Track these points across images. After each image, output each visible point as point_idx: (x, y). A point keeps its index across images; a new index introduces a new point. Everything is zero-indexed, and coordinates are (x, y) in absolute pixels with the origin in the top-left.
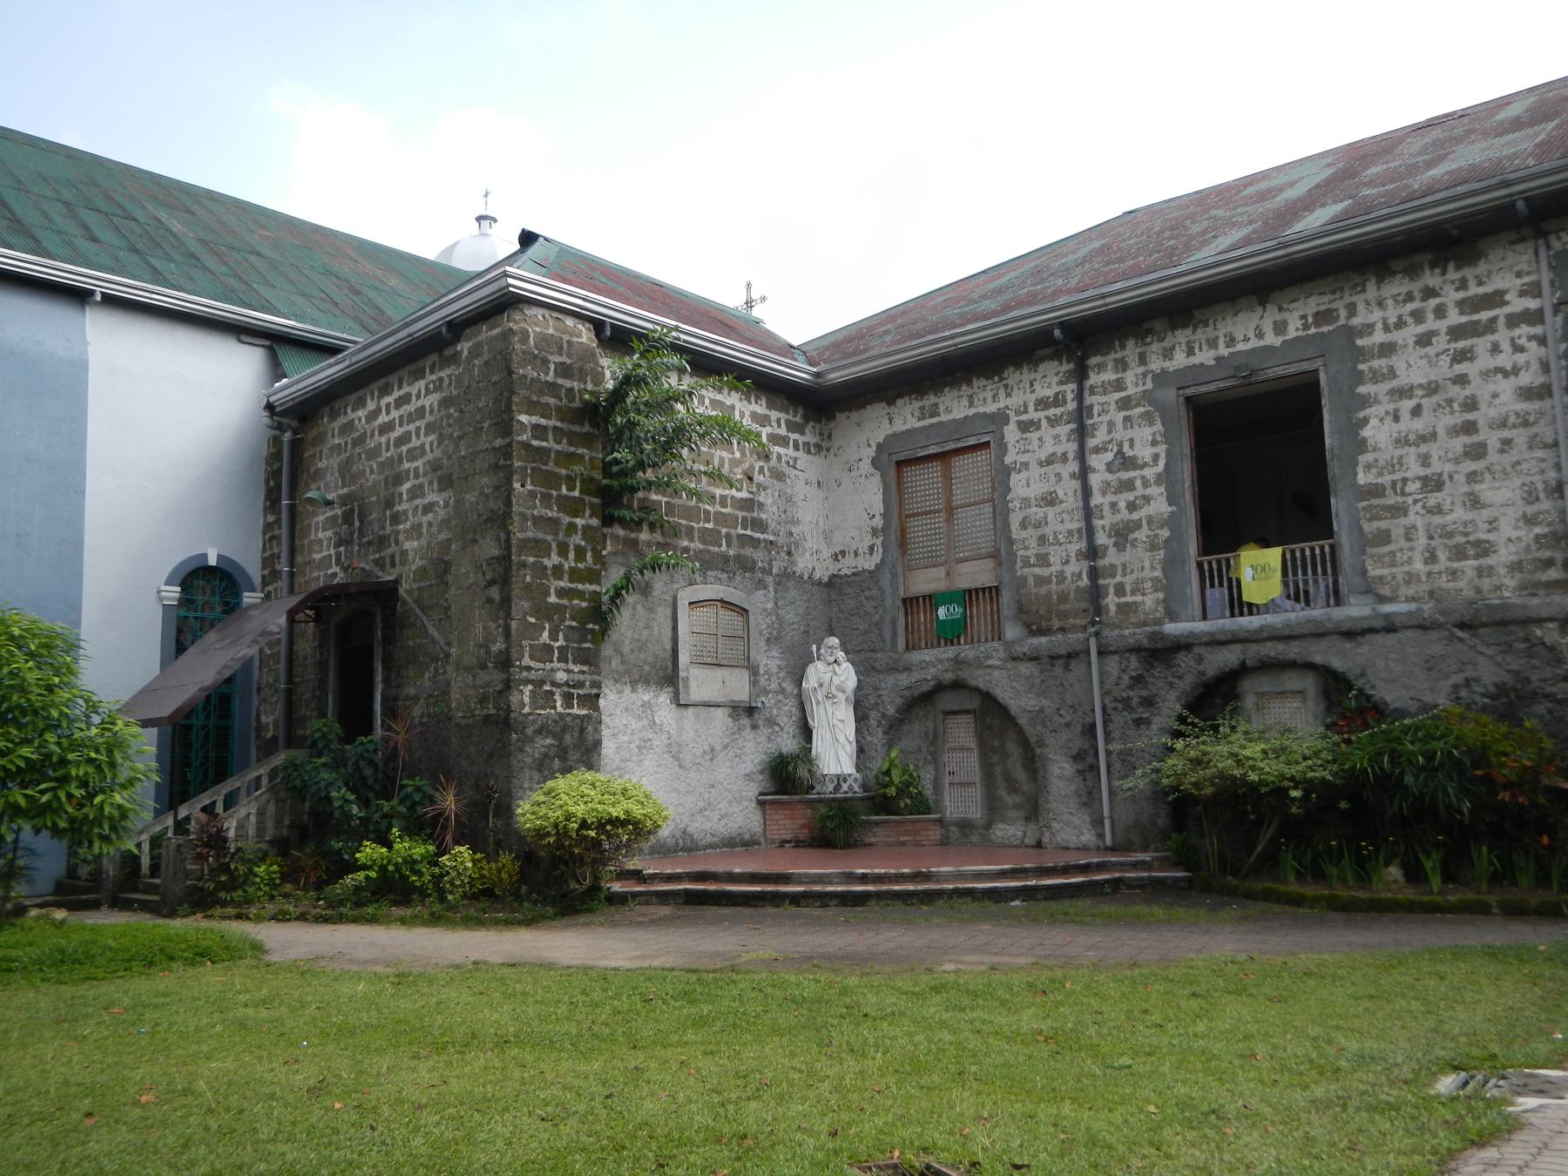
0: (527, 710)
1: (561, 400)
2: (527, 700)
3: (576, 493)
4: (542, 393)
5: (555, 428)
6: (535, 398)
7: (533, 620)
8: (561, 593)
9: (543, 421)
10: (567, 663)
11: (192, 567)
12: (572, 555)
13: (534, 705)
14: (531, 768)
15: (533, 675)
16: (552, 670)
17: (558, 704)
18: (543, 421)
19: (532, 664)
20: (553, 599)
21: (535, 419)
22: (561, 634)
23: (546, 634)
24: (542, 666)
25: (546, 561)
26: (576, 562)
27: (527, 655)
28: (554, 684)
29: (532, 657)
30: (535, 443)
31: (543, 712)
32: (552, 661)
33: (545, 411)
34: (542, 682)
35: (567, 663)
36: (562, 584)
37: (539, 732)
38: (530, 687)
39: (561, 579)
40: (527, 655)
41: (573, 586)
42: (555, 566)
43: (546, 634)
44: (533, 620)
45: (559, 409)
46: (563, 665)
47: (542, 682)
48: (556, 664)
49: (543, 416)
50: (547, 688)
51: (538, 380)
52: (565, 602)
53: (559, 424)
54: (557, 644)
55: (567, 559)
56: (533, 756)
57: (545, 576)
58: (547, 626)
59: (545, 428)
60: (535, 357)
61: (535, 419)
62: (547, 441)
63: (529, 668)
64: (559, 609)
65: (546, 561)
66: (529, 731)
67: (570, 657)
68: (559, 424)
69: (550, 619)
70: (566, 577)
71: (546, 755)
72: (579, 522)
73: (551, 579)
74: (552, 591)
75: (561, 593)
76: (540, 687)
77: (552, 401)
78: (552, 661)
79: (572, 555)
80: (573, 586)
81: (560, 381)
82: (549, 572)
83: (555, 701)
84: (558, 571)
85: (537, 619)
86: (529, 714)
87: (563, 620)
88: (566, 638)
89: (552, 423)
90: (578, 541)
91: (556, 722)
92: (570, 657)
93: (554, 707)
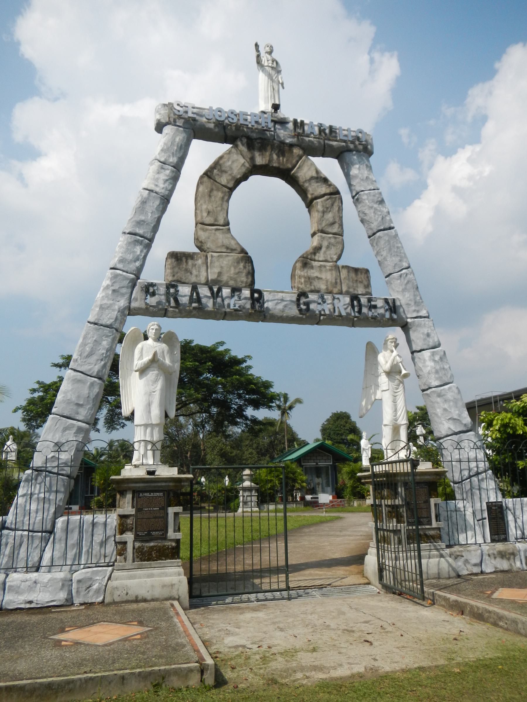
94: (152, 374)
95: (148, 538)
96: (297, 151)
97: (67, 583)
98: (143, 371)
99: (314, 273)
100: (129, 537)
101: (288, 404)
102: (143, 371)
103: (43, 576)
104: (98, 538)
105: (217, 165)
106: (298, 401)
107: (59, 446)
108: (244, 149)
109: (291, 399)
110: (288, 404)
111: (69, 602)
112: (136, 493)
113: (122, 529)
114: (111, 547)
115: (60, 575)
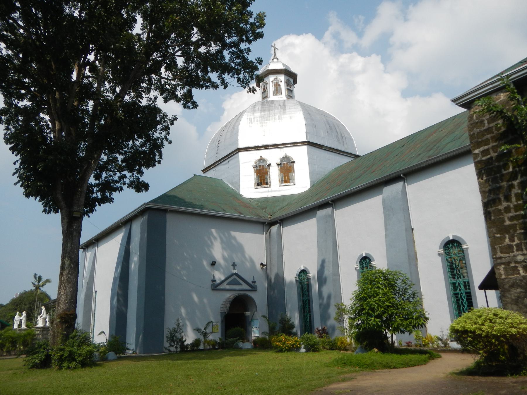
0: (503, 277)
1: (493, 133)
2: (502, 272)
3: (511, 170)
4: (483, 135)
5: (493, 146)
6: (480, 140)
7: (499, 235)
8: (511, 219)
9: (486, 147)
10: (522, 250)
11: (446, 241)
12: (514, 199)
13: (506, 273)
14: (510, 303)
15: (503, 260)
16: (514, 256)
17: (521, 271)
18: (486, 147)
19: (502, 255)
20: (508, 223)
21: (482, 149)
22: (516, 239)
23: (507, 240)
24: (508, 255)
25: (501, 207)
26: (517, 201)
27: (498, 252)
28: (516, 262)
29: (501, 252)
30: (484, 158)
31: (512, 277)
32: (513, 252)
33: (486, 143)
34: (509, 263)
35: (522, 250)
36: (511, 214)
37: (512, 286)
38: (503, 266)
39: (510, 212)
40: (498, 252)
41: (518, 213)
42: (505, 208)
43: (507, 240)
44: (499, 235)
45: (492, 138)
46: (520, 252)
47: (509, 263)
48: (516, 253)
49: (485, 145)
50: (513, 265)
51: (481, 131)
52: (515, 222)
53: (495, 144)
54: (515, 243)
55: (511, 202)
56: (511, 298)
57: (502, 214)
58: (507, 236)
59: (488, 150)
60: (477, 123)
61: (482, 149)
62: (489, 154)
63: (501, 258)
64: (510, 227)
65: (501, 207)
66: (507, 286)
67: (523, 247)
68: (495, 144)
69: (508, 232)
70: (512, 210)
71: (519, 297)
72: (515, 183)
73: (505, 214)
74: (506, 219)
75: (511, 219)
76: (509, 265)
77: (489, 136)
78: (513, 252)
79: (514, 199)
80: (518, 213)
81: (491, 125)
82: (503, 211)
83: (519, 270)
84: (507, 210)
85: (500, 234)
86: (505, 279)
87: (515, 231)
88: (519, 239)
89: (490, 146)
90: (516, 191)
91: (521, 281)
92: (523, 247)
93: (519, 274)
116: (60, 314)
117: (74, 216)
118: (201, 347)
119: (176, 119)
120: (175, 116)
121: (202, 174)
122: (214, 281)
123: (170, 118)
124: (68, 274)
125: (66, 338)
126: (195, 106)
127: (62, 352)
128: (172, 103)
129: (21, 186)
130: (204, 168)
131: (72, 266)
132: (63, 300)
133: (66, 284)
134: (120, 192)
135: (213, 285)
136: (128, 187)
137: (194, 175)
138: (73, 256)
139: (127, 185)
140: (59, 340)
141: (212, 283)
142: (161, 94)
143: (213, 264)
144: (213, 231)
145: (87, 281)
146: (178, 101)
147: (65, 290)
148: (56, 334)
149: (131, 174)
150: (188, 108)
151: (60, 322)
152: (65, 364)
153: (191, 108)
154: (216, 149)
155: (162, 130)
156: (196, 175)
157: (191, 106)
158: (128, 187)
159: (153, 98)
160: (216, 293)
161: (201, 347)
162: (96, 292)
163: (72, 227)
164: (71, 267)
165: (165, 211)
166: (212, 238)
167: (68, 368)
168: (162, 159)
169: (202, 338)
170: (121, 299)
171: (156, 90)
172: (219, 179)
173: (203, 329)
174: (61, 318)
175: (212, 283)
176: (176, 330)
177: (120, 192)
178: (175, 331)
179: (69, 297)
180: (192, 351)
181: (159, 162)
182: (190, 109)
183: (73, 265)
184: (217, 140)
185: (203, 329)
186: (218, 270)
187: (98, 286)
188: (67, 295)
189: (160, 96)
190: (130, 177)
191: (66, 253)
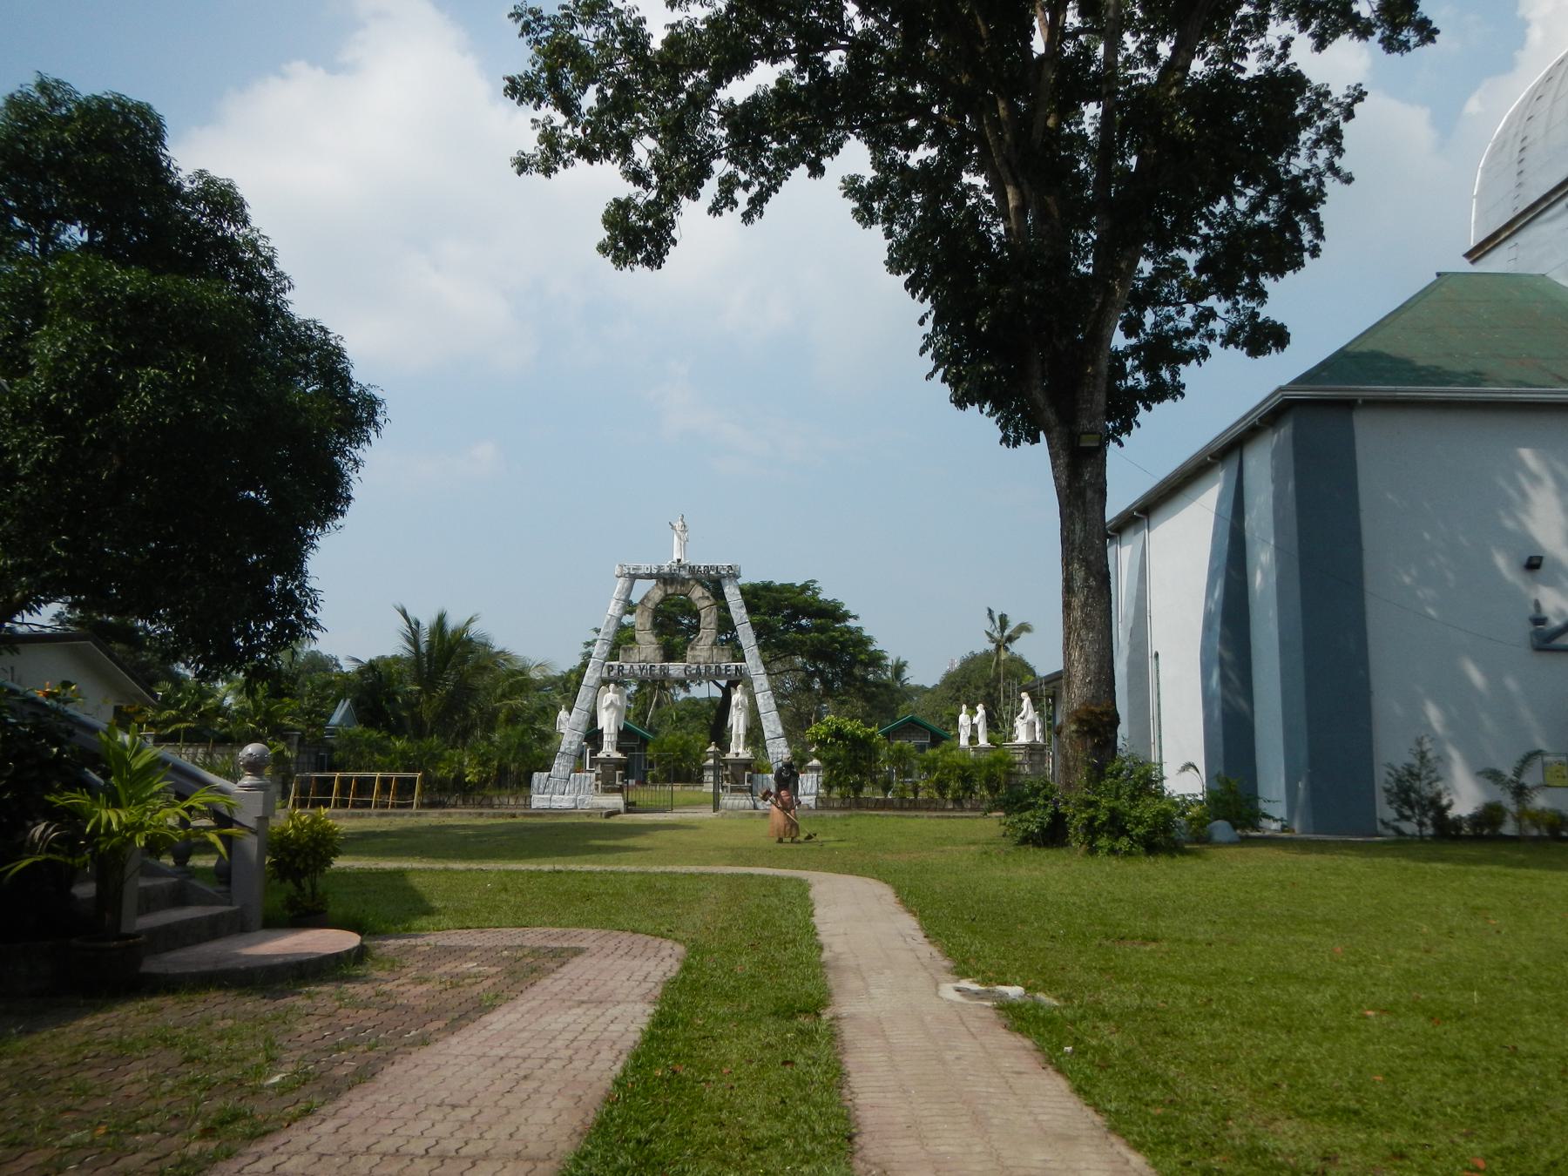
94: (611, 710)
95: (607, 783)
96: (691, 582)
97: (575, 800)
98: (607, 708)
99: (697, 653)
100: (599, 783)
101: (1007, 633)
102: (607, 708)
103: (566, 797)
104: (588, 782)
105: (646, 597)
106: (1024, 628)
107: (570, 743)
108: (661, 586)
109: (1013, 624)
110: (1007, 633)
111: (576, 808)
112: (602, 764)
113: (597, 779)
114: (593, 787)
115: (572, 797)
116: (1076, 711)
117: (1082, 445)
118: (1509, 829)
119: (1360, 96)
120: (1355, 89)
121: (1466, 266)
122: (1539, 620)
123: (1341, 100)
124: (1084, 605)
125: (1098, 774)
126: (1427, 32)
127: (1091, 811)
128: (1345, 46)
129: (944, 380)
130: (1473, 244)
131: (1093, 583)
132: (1079, 675)
133: (1083, 632)
134: (1200, 364)
135: (1536, 634)
136: (1221, 345)
137: (1439, 274)
138: (1092, 558)
139: (1219, 340)
140: (1081, 777)
141: (1532, 628)
142: (1304, 26)
143: (1533, 564)
144: (1527, 454)
145: (1130, 625)
146: (1363, 30)
147: (1081, 648)
148: (1072, 764)
149: (1228, 304)
150: (1404, 46)
151: (1077, 732)
152: (1103, 842)
153: (1411, 44)
154: (1515, 168)
155: (1316, 143)
156: (1446, 274)
157: (1414, 40)
158: (1221, 345)
159: (1278, 44)
160: (1548, 658)
161: (1509, 829)
162: (1157, 655)
163: (1082, 475)
164: (1089, 587)
165: (1348, 405)
166: (1524, 481)
167: (1113, 851)
168: (1323, 238)
169: (1508, 801)
170: (1232, 675)
171: (1285, 18)
172: (1531, 276)
173: (1509, 773)
174: (1080, 721)
175: (1532, 628)
176: (1416, 770)
177: (1200, 364)
178: (1411, 774)
179: (1092, 667)
180: (1477, 838)
181: (1315, 252)
182: (1409, 49)
183: (1095, 579)
184: (1516, 135)
185: (1509, 773)
186: (1552, 583)
187: (1158, 640)
188: (1087, 660)
189: (1301, 31)
190: (1227, 312)
191: (1072, 551)
